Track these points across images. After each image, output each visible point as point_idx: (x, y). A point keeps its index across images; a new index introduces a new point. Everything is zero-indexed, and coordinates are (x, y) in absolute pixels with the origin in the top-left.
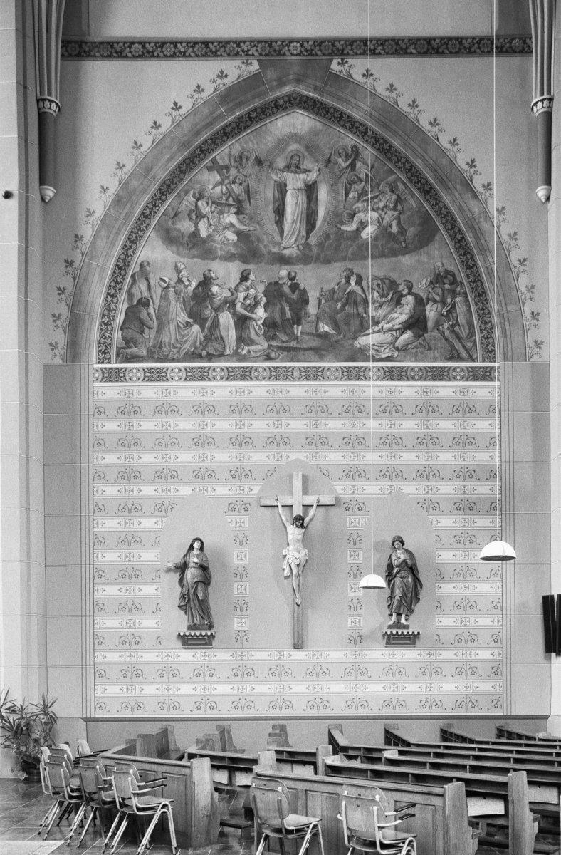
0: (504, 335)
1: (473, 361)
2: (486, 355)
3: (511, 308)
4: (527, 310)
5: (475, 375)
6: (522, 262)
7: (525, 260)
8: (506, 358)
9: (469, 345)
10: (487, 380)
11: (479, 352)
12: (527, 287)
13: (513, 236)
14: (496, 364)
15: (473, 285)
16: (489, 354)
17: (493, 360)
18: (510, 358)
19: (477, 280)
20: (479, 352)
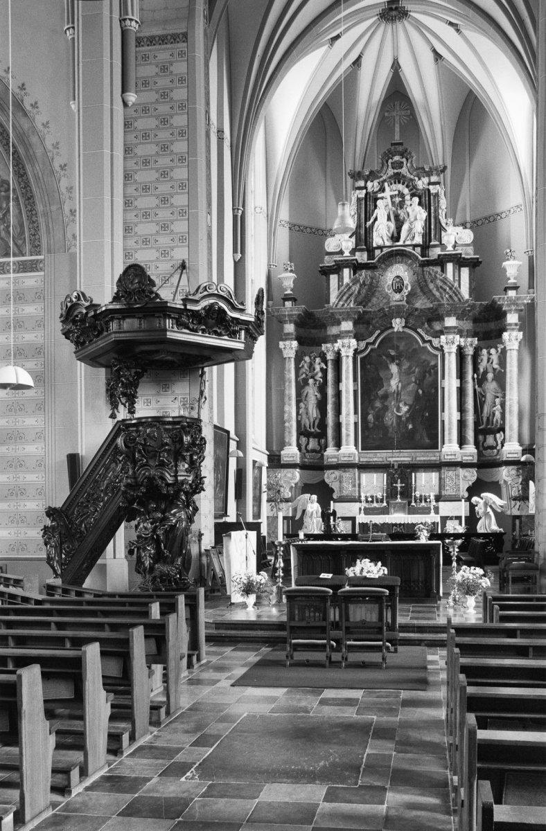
0: (48, 232)
1: (23, 255)
2: (33, 250)
3: (54, 208)
4: (67, 209)
5: (24, 267)
6: (63, 167)
7: (65, 165)
8: (49, 251)
9: (20, 242)
10: (34, 271)
11: (28, 247)
12: (67, 188)
13: (56, 146)
14: (42, 257)
15: (24, 191)
16: (36, 249)
17: (39, 253)
18: (52, 252)
19: (27, 186)
20: (28, 247)
